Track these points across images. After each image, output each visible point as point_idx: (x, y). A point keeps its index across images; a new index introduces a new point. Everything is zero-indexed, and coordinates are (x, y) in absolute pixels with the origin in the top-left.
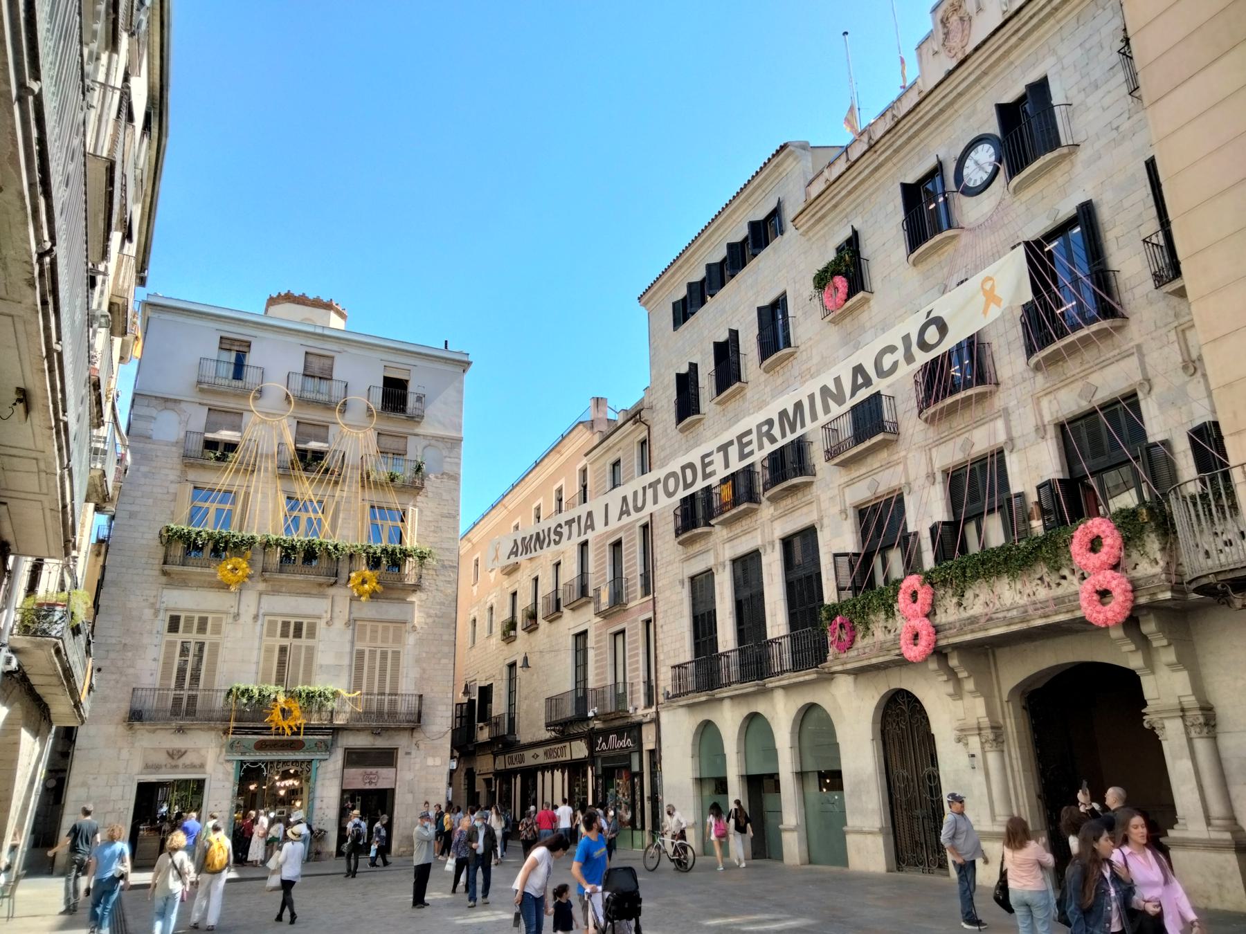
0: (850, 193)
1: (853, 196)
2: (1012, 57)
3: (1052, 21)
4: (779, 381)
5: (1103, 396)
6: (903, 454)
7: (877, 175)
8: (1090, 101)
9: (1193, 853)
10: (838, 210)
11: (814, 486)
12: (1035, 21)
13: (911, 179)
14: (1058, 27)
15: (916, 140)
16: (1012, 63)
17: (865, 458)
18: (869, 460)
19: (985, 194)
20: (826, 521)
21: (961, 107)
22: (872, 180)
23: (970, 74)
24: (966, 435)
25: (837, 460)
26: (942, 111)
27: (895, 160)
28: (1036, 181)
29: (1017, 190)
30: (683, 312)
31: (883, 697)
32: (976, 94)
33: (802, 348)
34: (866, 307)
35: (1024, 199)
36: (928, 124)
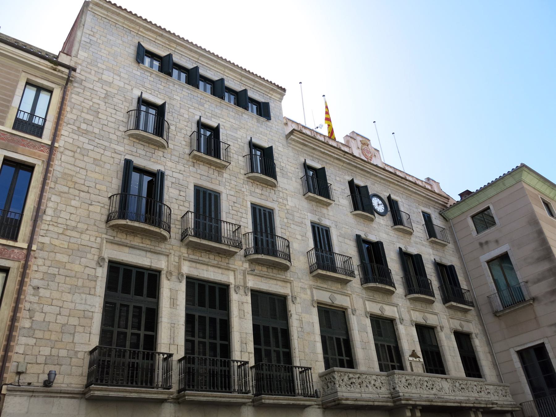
0: (324, 153)
1: (322, 155)
2: (391, 185)
3: (402, 190)
7: (336, 161)
10: (314, 151)
15: (355, 169)
16: (389, 186)
18: (330, 283)
20: (298, 299)
22: (332, 160)
23: (383, 175)
26: (368, 172)
27: (344, 165)
36: (362, 170)
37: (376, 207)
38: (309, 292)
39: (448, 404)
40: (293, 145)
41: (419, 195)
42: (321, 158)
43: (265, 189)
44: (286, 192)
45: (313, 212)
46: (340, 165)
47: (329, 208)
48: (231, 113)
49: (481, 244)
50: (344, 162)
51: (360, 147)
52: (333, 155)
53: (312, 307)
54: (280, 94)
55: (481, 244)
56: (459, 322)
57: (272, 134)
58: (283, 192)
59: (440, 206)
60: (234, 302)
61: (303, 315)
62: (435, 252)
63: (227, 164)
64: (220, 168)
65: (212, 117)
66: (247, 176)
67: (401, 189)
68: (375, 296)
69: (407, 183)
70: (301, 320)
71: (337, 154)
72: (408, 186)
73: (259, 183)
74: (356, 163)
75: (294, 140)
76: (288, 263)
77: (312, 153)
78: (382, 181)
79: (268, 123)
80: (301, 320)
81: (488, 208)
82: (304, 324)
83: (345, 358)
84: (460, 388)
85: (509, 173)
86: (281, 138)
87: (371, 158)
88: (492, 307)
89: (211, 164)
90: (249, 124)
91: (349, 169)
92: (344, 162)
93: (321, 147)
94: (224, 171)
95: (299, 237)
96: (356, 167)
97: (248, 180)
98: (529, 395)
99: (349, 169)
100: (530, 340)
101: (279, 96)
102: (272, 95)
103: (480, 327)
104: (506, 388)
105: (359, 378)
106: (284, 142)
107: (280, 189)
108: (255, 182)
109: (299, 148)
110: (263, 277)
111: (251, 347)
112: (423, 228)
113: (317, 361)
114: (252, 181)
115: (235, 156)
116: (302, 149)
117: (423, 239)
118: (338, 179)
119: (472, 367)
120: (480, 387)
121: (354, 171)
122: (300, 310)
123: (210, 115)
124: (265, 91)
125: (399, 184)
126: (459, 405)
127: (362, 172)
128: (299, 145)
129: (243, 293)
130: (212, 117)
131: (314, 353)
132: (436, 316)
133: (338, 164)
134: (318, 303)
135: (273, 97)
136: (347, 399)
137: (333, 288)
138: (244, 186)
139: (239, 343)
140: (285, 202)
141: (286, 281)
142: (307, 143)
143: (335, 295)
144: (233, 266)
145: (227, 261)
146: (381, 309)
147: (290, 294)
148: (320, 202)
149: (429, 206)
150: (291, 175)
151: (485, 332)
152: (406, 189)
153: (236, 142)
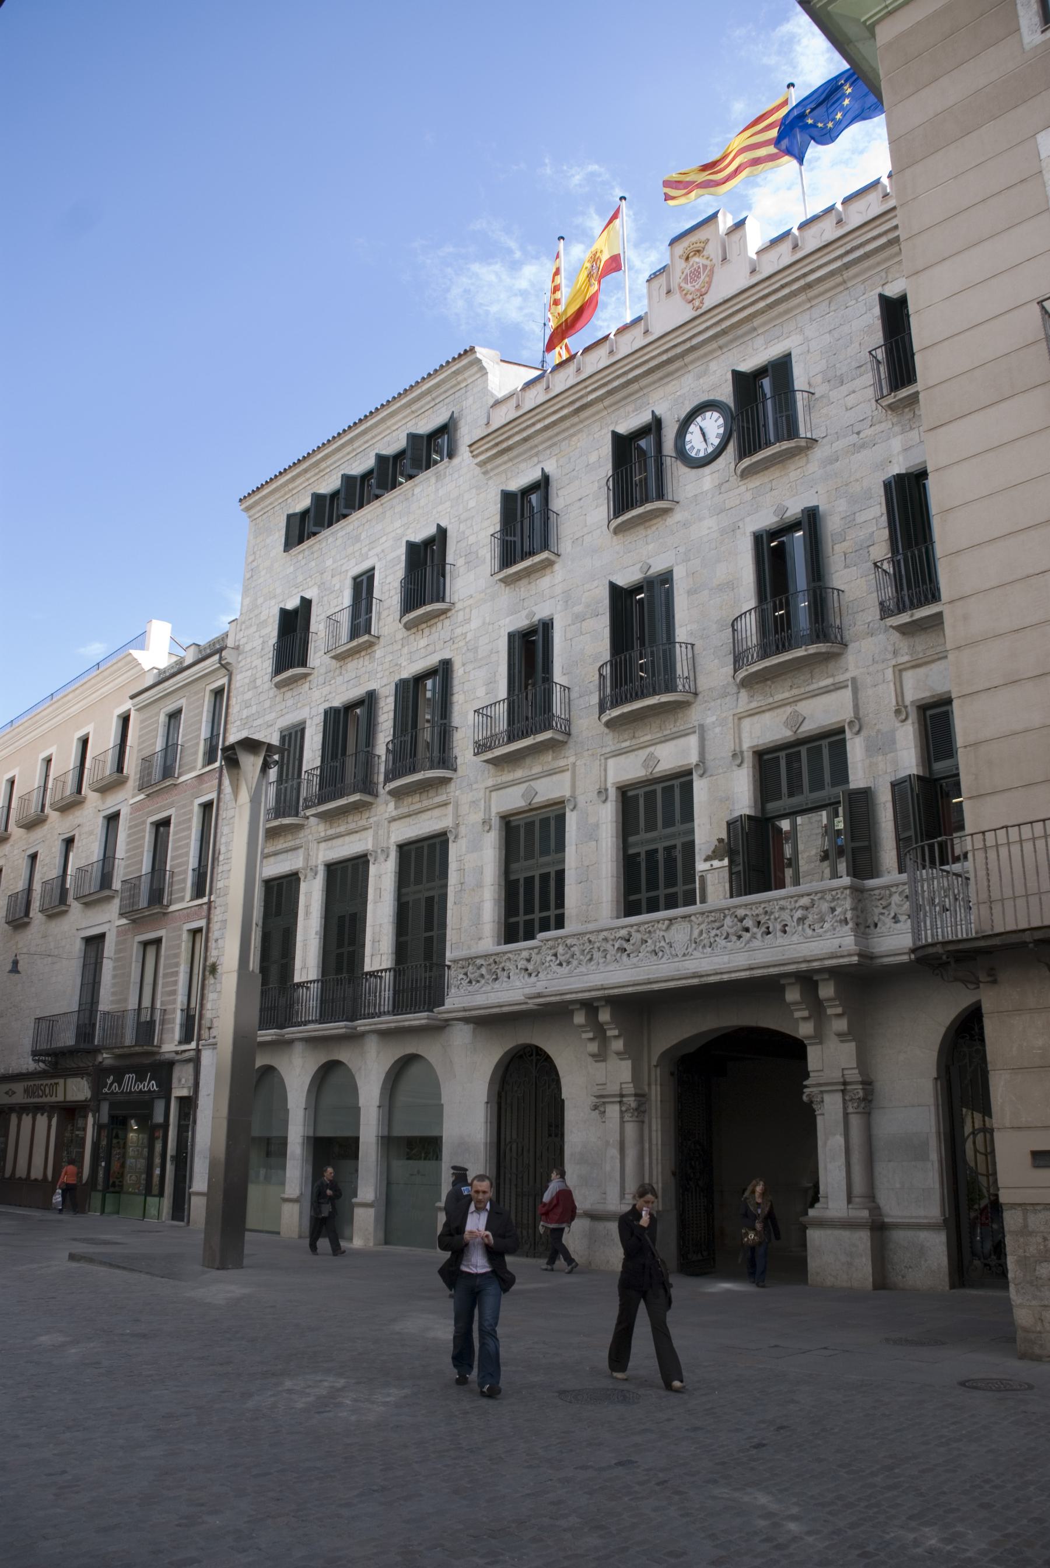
0: (547, 428)
2: (756, 322)
3: (802, 297)
4: (423, 643)
5: (808, 728)
6: (572, 759)
8: (834, 395)
9: (829, 1232)
11: (453, 785)
12: (786, 291)
13: (623, 429)
14: (809, 305)
15: (635, 386)
16: (755, 329)
17: (524, 758)
19: (707, 470)
20: (463, 830)
21: (692, 362)
22: (575, 419)
23: (707, 329)
25: (489, 755)
27: (606, 403)
28: (767, 468)
29: (745, 474)
30: (302, 529)
31: (506, 1053)
33: (459, 606)
34: (548, 571)
35: (751, 485)
40: (492, 469)
41: (867, 256)
43: (434, 629)
44: (471, 601)
46: (598, 413)
54: (471, 364)
77: (532, 448)
78: (722, 341)
89: (359, 652)
91: (625, 398)
93: (534, 424)
99: (625, 398)
101: (475, 369)
102: (465, 379)
109: (505, 463)
113: (480, 939)
121: (637, 392)
124: (452, 387)
128: (499, 461)
131: (477, 922)
133: (594, 415)
135: (469, 381)
146: (651, 760)
152: (809, 286)
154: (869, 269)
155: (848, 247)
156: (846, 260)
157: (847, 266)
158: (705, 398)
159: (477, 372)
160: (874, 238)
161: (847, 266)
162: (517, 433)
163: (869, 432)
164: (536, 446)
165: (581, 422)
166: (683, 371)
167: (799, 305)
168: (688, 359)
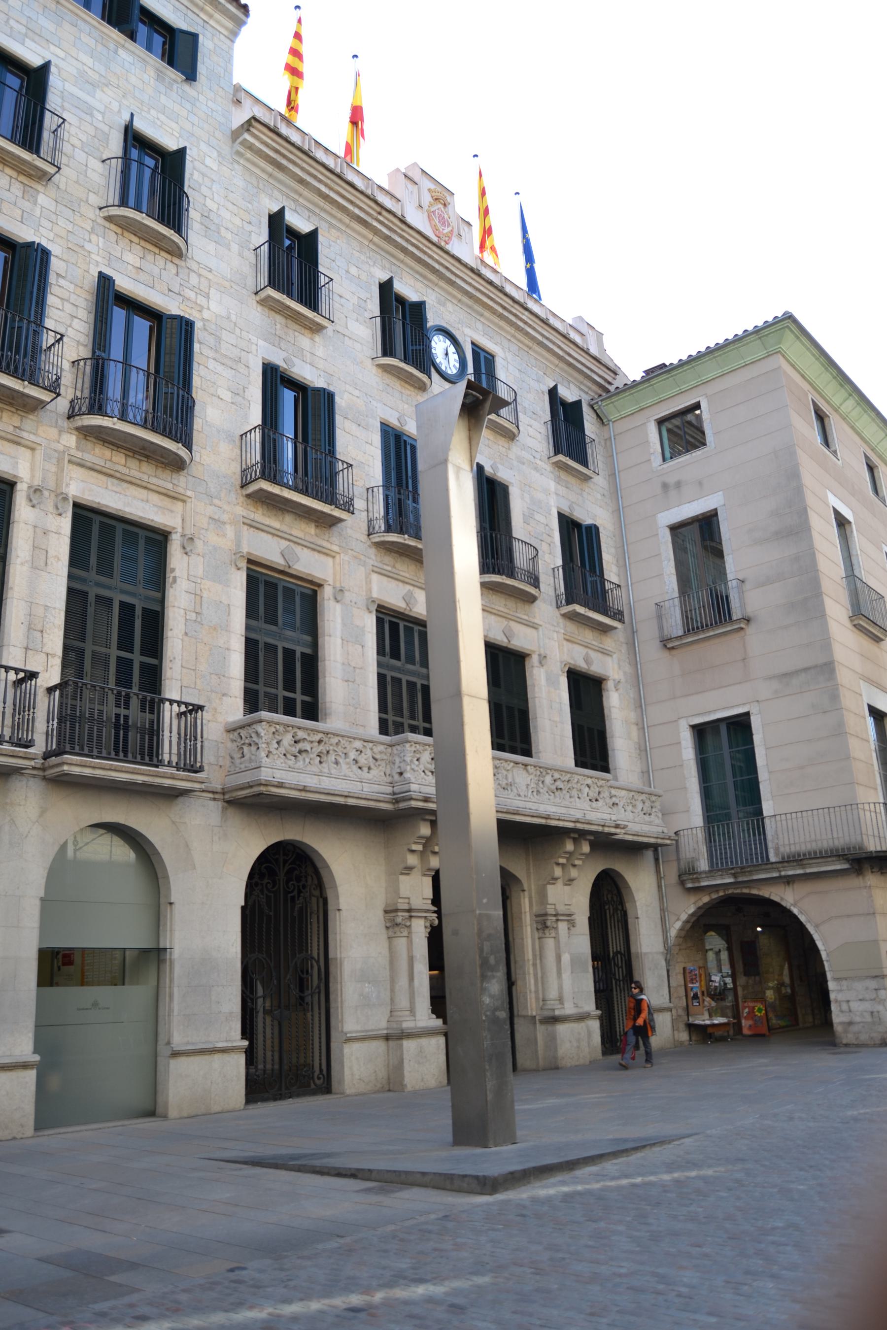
0: (326, 197)
3: (512, 330)
10: (300, 188)
15: (401, 256)
16: (482, 315)
18: (288, 518)
20: (199, 543)
22: (347, 220)
24: (411, 588)
27: (376, 239)
32: (454, 297)
36: (419, 261)
37: (440, 359)
38: (230, 531)
39: (518, 818)
40: (248, 160)
42: (317, 211)
43: (150, 257)
44: (210, 276)
45: (275, 340)
46: (364, 237)
47: (317, 338)
48: (85, 39)
49: (665, 486)
50: (376, 232)
51: (426, 207)
52: (350, 207)
53: (233, 569)
55: (665, 486)
56: (583, 651)
57: (195, 120)
58: (200, 275)
59: (595, 388)
60: (22, 525)
61: (207, 584)
62: (562, 490)
63: (51, 170)
64: (29, 176)
65: (26, 35)
66: (105, 212)
67: (508, 328)
68: (398, 566)
69: (525, 316)
70: (197, 596)
71: (360, 208)
72: (526, 323)
73: (136, 240)
74: (407, 240)
75: (251, 147)
76: (182, 452)
77: (296, 192)
78: (465, 299)
79: (186, 87)
80: (197, 596)
81: (697, 406)
82: (205, 606)
83: (299, 697)
84: (554, 787)
85: (757, 331)
86: (218, 134)
87: (450, 238)
88: (661, 628)
90: (133, 80)
92: (376, 232)
93: (320, 181)
94: (39, 187)
95: (227, 396)
96: (404, 250)
97: (107, 224)
98: (693, 815)
100: (720, 706)
101: (230, 24)
102: (211, 16)
103: (628, 668)
104: (654, 798)
105: (320, 742)
106: (226, 149)
107: (194, 266)
108: (126, 234)
109: (263, 171)
110: (111, 476)
111: (55, 641)
112: (543, 430)
113: (224, 695)
114: (119, 231)
115: (80, 156)
116: (271, 175)
117: (538, 456)
118: (353, 270)
119: (592, 748)
120: (597, 790)
121: (398, 259)
122: (200, 572)
123: (24, 30)
125: (506, 314)
126: (543, 821)
127: (418, 267)
128: (262, 163)
129: (51, 509)
130: (26, 35)
131: (222, 675)
132: (534, 631)
133: (359, 234)
134: (250, 561)
135: (212, 22)
136: (281, 785)
137: (295, 532)
138: (94, 238)
139: (23, 629)
140: (201, 300)
141: (174, 497)
142: (284, 162)
143: (298, 549)
144: (32, 438)
145: (16, 420)
147: (180, 530)
148: (296, 317)
149: (569, 382)
150: (229, 236)
151: (637, 680)
153: (88, 118)
154: (543, 356)
155: (551, 337)
156: (545, 341)
157: (540, 344)
158: (445, 325)
159: (226, 28)
160: (559, 347)
161: (540, 344)
162: (302, 169)
163: (538, 462)
164: (301, 195)
165: (347, 226)
166: (430, 285)
167: (507, 332)
168: (442, 283)
